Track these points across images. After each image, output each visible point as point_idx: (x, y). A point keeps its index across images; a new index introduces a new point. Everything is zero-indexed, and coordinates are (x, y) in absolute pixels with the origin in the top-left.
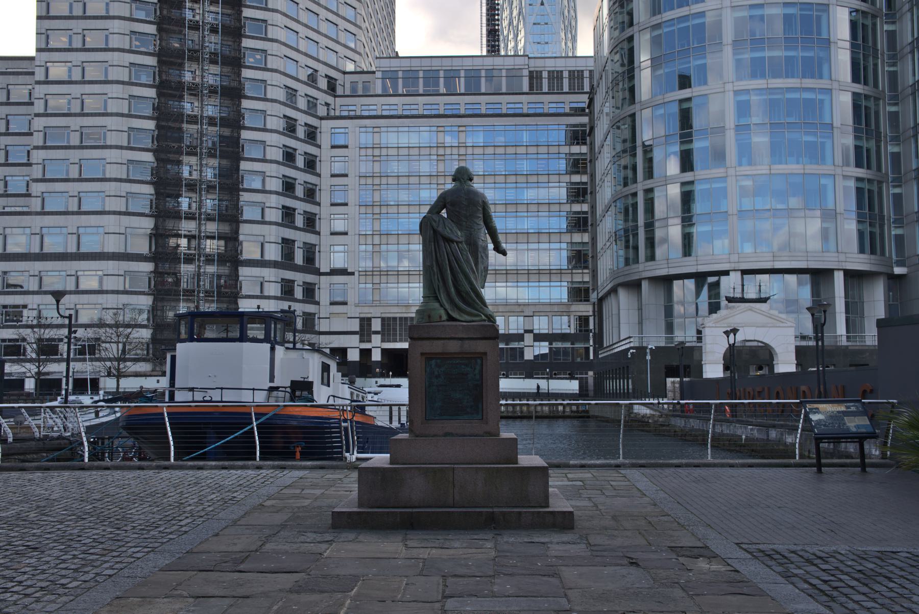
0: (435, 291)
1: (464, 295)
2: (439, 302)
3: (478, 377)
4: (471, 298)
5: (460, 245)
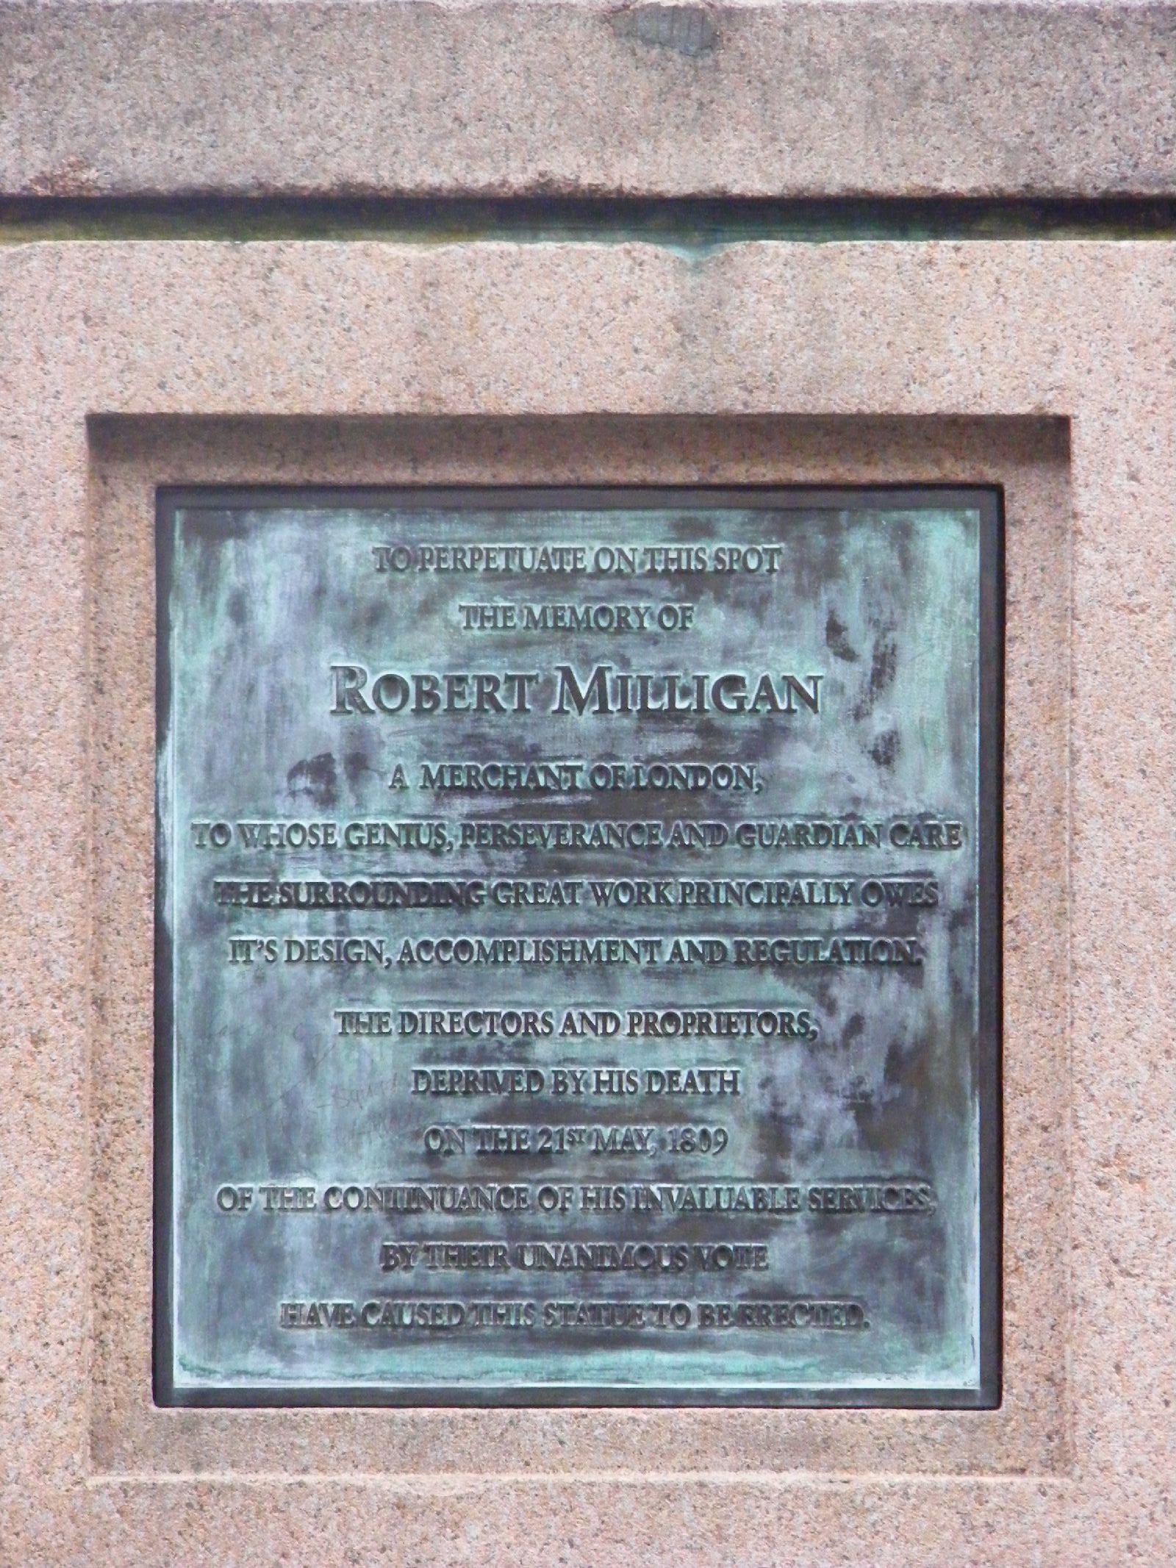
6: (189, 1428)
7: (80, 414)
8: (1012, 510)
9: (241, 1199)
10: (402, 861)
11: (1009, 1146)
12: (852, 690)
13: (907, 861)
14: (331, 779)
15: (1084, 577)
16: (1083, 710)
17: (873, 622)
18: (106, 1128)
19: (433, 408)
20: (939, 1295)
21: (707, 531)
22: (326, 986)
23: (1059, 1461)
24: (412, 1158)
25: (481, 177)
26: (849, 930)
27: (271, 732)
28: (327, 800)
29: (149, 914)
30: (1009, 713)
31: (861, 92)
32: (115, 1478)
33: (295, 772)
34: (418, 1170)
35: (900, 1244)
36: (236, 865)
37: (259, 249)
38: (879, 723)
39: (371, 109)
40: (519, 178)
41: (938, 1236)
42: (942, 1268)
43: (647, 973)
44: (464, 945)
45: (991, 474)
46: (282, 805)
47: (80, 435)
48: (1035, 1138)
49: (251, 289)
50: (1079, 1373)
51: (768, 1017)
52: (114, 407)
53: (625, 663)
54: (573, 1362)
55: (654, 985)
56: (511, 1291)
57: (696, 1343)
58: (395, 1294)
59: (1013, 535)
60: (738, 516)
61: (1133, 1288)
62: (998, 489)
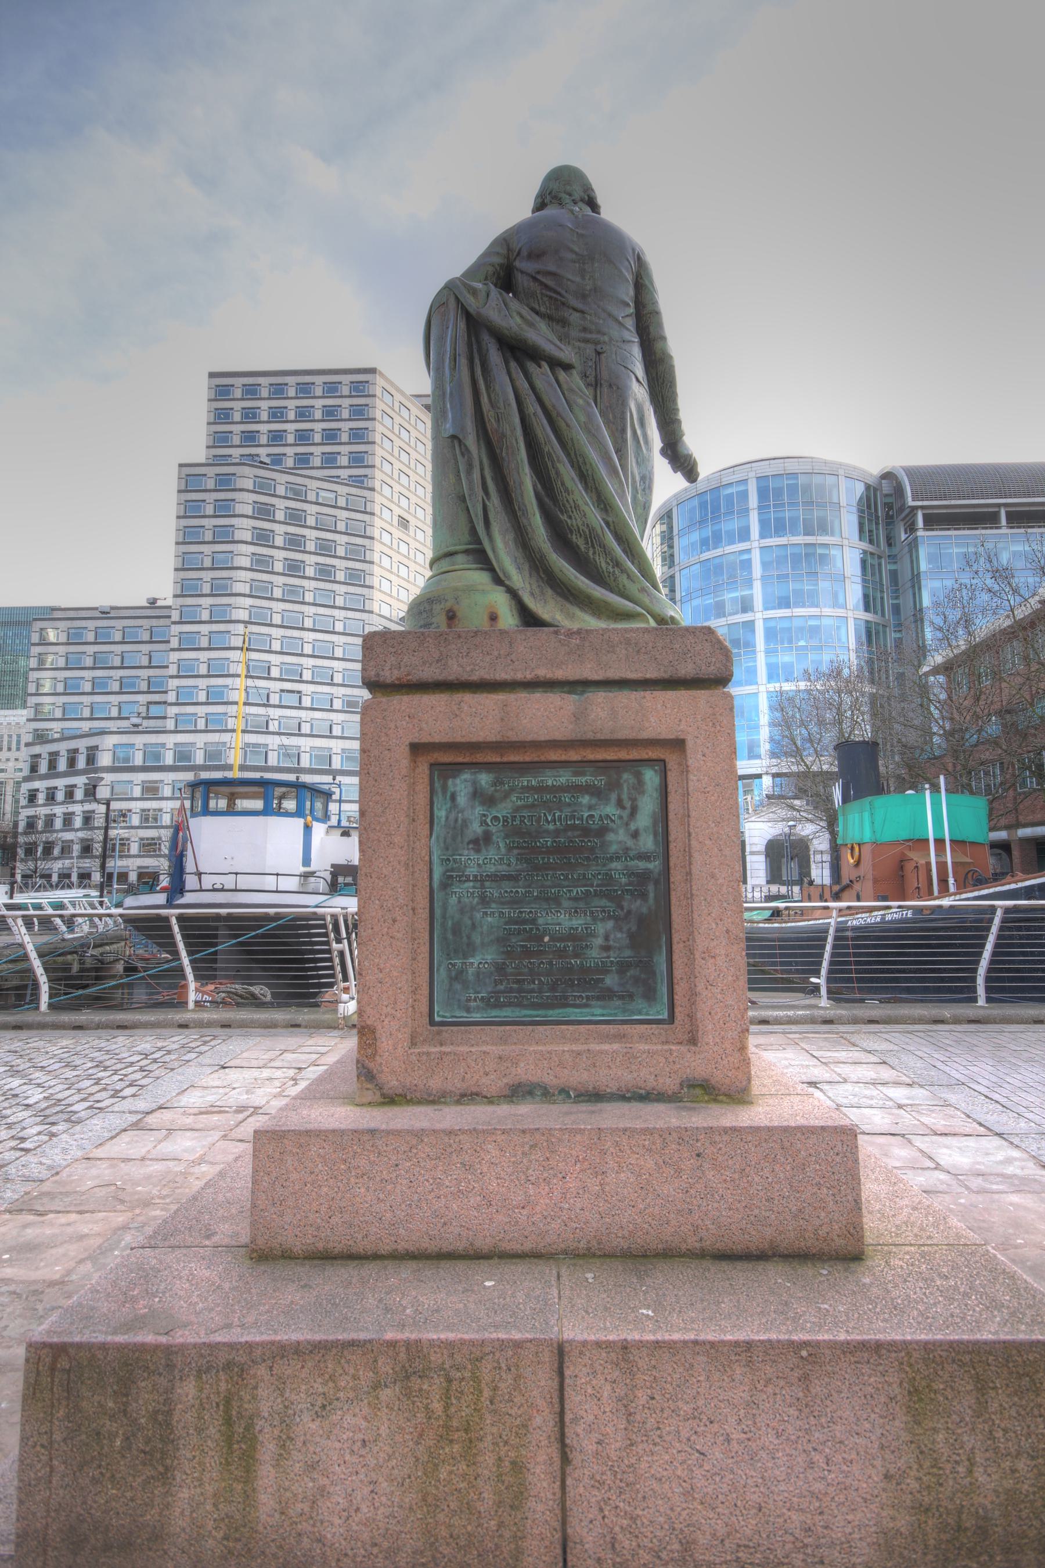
0: (473, 531)
1: (581, 543)
2: (491, 569)
3: (647, 842)
4: (607, 551)
5: (562, 375)
6: (439, 1033)
7: (407, 743)
8: (669, 767)
9: (454, 965)
10: (500, 868)
11: (674, 947)
12: (625, 818)
13: (642, 865)
14: (479, 845)
15: (691, 784)
16: (693, 821)
17: (630, 799)
18: (415, 946)
19: (506, 739)
20: (655, 990)
21: (583, 774)
22: (478, 904)
23: (693, 1041)
24: (503, 952)
25: (519, 676)
26: (626, 885)
27: (462, 831)
28: (478, 851)
29: (427, 883)
30: (670, 823)
31: (624, 652)
32: (417, 1051)
33: (468, 843)
34: (503, 956)
35: (643, 976)
36: (452, 870)
37: (458, 697)
38: (633, 827)
39: (488, 659)
40: (529, 676)
41: (654, 973)
42: (656, 983)
43: (570, 899)
44: (517, 892)
45: (662, 757)
46: (466, 852)
47: (407, 749)
48: (682, 945)
49: (455, 708)
50: (699, 1015)
51: (604, 911)
52: (417, 741)
53: (561, 811)
54: (551, 1012)
55: (571, 902)
56: (532, 991)
57: (586, 1006)
58: (499, 992)
59: (669, 773)
60: (592, 769)
61: (715, 990)
62: (664, 761)
